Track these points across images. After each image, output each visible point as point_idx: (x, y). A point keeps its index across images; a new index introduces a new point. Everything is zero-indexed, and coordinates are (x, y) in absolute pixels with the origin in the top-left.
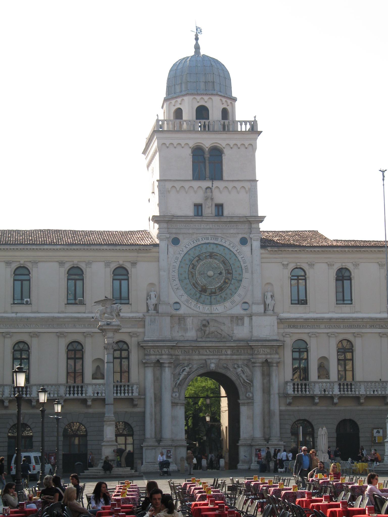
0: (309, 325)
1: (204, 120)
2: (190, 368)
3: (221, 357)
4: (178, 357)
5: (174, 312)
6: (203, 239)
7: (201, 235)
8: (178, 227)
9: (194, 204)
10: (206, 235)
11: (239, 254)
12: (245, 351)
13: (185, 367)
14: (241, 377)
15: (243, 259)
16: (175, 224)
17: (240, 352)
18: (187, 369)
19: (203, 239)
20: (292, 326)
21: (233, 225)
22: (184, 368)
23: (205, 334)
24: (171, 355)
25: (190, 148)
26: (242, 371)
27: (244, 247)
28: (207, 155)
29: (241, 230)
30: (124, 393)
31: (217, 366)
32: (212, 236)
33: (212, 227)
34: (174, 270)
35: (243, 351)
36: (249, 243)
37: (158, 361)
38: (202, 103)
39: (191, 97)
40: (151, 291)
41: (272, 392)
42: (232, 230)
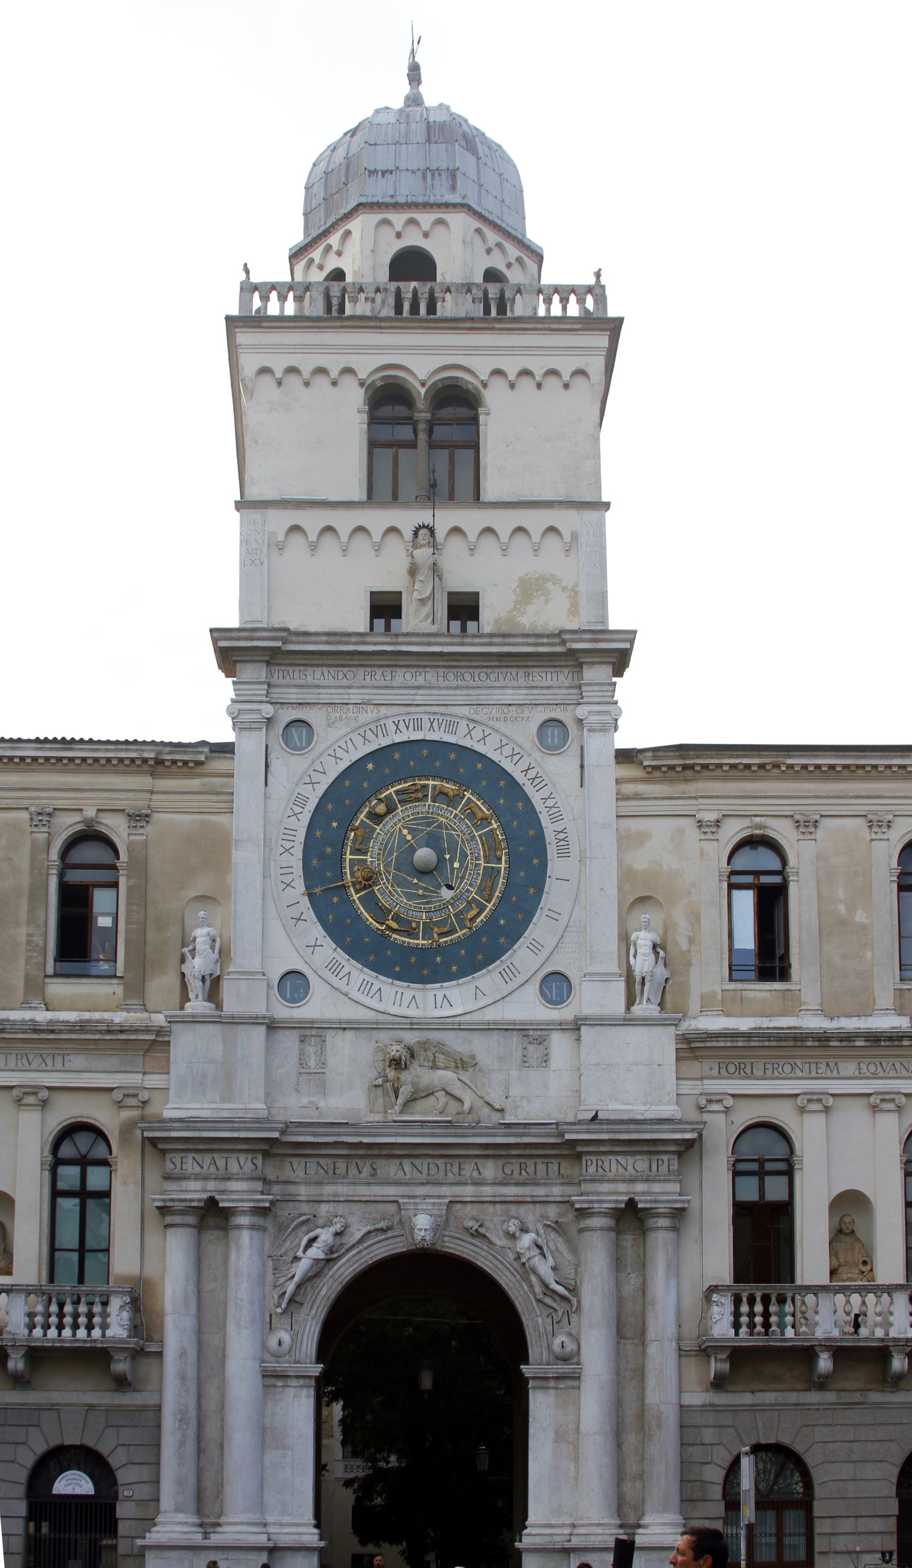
0: (799, 1062)
1: (413, 284)
2: (337, 1234)
3: (458, 1190)
4: (291, 1189)
5: (282, 1011)
6: (402, 726)
7: (395, 710)
8: (310, 679)
9: (372, 594)
10: (412, 709)
11: (534, 785)
12: (554, 1168)
13: (317, 1227)
14: (534, 1271)
15: (550, 803)
16: (297, 669)
17: (531, 1169)
18: (326, 1236)
19: (402, 726)
20: (732, 1069)
21: (514, 671)
22: (312, 1235)
23: (397, 1098)
24: (265, 1181)
25: (362, 384)
26: (539, 1247)
27: (553, 758)
28: (423, 413)
29: (545, 692)
30: (75, 1326)
31: (439, 1228)
32: (435, 717)
33: (434, 680)
34: (288, 845)
35: (541, 1167)
36: (572, 746)
37: (212, 1202)
38: (413, 239)
39: (377, 217)
40: (197, 927)
41: (651, 1334)
42: (510, 691)
